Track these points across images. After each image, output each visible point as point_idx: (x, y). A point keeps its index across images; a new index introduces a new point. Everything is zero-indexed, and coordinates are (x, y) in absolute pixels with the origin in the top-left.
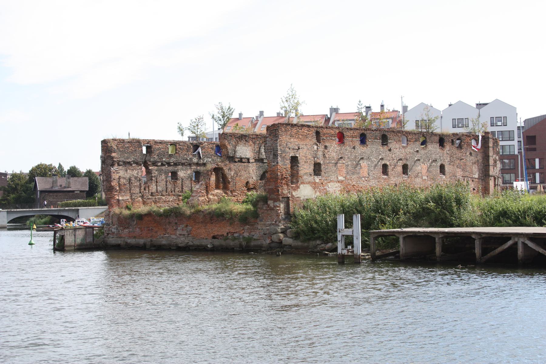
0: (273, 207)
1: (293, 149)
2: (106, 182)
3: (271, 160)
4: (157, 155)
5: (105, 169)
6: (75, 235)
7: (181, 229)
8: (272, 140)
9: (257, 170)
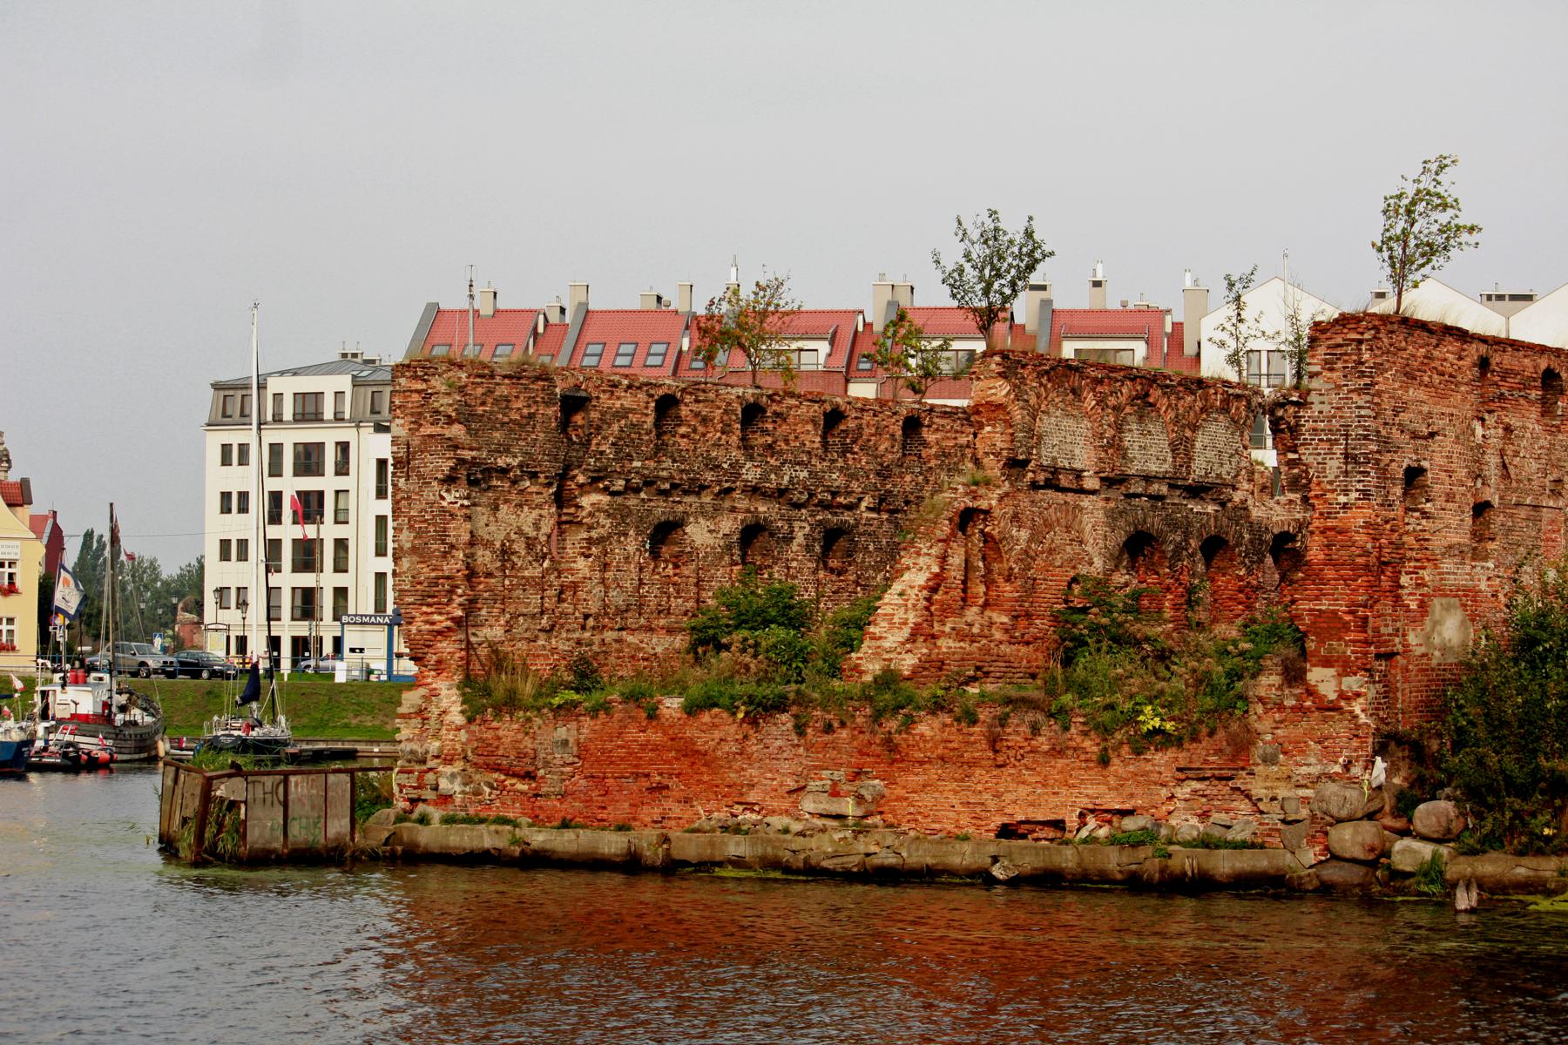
0: (1333, 696)
1: (1415, 436)
2: (415, 558)
3: (1331, 483)
4: (613, 444)
5: (409, 498)
6: (285, 805)
7: (827, 788)
8: (1339, 387)
9: (1108, 525)
